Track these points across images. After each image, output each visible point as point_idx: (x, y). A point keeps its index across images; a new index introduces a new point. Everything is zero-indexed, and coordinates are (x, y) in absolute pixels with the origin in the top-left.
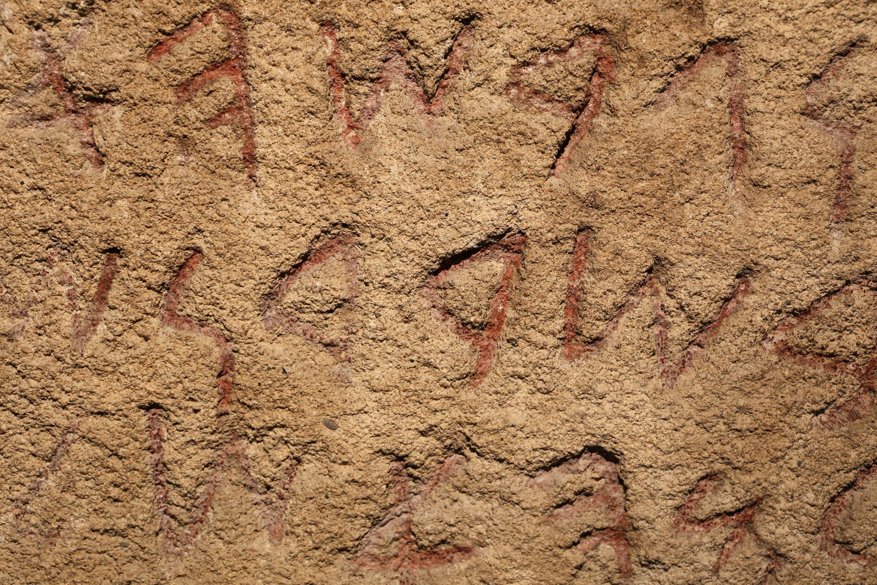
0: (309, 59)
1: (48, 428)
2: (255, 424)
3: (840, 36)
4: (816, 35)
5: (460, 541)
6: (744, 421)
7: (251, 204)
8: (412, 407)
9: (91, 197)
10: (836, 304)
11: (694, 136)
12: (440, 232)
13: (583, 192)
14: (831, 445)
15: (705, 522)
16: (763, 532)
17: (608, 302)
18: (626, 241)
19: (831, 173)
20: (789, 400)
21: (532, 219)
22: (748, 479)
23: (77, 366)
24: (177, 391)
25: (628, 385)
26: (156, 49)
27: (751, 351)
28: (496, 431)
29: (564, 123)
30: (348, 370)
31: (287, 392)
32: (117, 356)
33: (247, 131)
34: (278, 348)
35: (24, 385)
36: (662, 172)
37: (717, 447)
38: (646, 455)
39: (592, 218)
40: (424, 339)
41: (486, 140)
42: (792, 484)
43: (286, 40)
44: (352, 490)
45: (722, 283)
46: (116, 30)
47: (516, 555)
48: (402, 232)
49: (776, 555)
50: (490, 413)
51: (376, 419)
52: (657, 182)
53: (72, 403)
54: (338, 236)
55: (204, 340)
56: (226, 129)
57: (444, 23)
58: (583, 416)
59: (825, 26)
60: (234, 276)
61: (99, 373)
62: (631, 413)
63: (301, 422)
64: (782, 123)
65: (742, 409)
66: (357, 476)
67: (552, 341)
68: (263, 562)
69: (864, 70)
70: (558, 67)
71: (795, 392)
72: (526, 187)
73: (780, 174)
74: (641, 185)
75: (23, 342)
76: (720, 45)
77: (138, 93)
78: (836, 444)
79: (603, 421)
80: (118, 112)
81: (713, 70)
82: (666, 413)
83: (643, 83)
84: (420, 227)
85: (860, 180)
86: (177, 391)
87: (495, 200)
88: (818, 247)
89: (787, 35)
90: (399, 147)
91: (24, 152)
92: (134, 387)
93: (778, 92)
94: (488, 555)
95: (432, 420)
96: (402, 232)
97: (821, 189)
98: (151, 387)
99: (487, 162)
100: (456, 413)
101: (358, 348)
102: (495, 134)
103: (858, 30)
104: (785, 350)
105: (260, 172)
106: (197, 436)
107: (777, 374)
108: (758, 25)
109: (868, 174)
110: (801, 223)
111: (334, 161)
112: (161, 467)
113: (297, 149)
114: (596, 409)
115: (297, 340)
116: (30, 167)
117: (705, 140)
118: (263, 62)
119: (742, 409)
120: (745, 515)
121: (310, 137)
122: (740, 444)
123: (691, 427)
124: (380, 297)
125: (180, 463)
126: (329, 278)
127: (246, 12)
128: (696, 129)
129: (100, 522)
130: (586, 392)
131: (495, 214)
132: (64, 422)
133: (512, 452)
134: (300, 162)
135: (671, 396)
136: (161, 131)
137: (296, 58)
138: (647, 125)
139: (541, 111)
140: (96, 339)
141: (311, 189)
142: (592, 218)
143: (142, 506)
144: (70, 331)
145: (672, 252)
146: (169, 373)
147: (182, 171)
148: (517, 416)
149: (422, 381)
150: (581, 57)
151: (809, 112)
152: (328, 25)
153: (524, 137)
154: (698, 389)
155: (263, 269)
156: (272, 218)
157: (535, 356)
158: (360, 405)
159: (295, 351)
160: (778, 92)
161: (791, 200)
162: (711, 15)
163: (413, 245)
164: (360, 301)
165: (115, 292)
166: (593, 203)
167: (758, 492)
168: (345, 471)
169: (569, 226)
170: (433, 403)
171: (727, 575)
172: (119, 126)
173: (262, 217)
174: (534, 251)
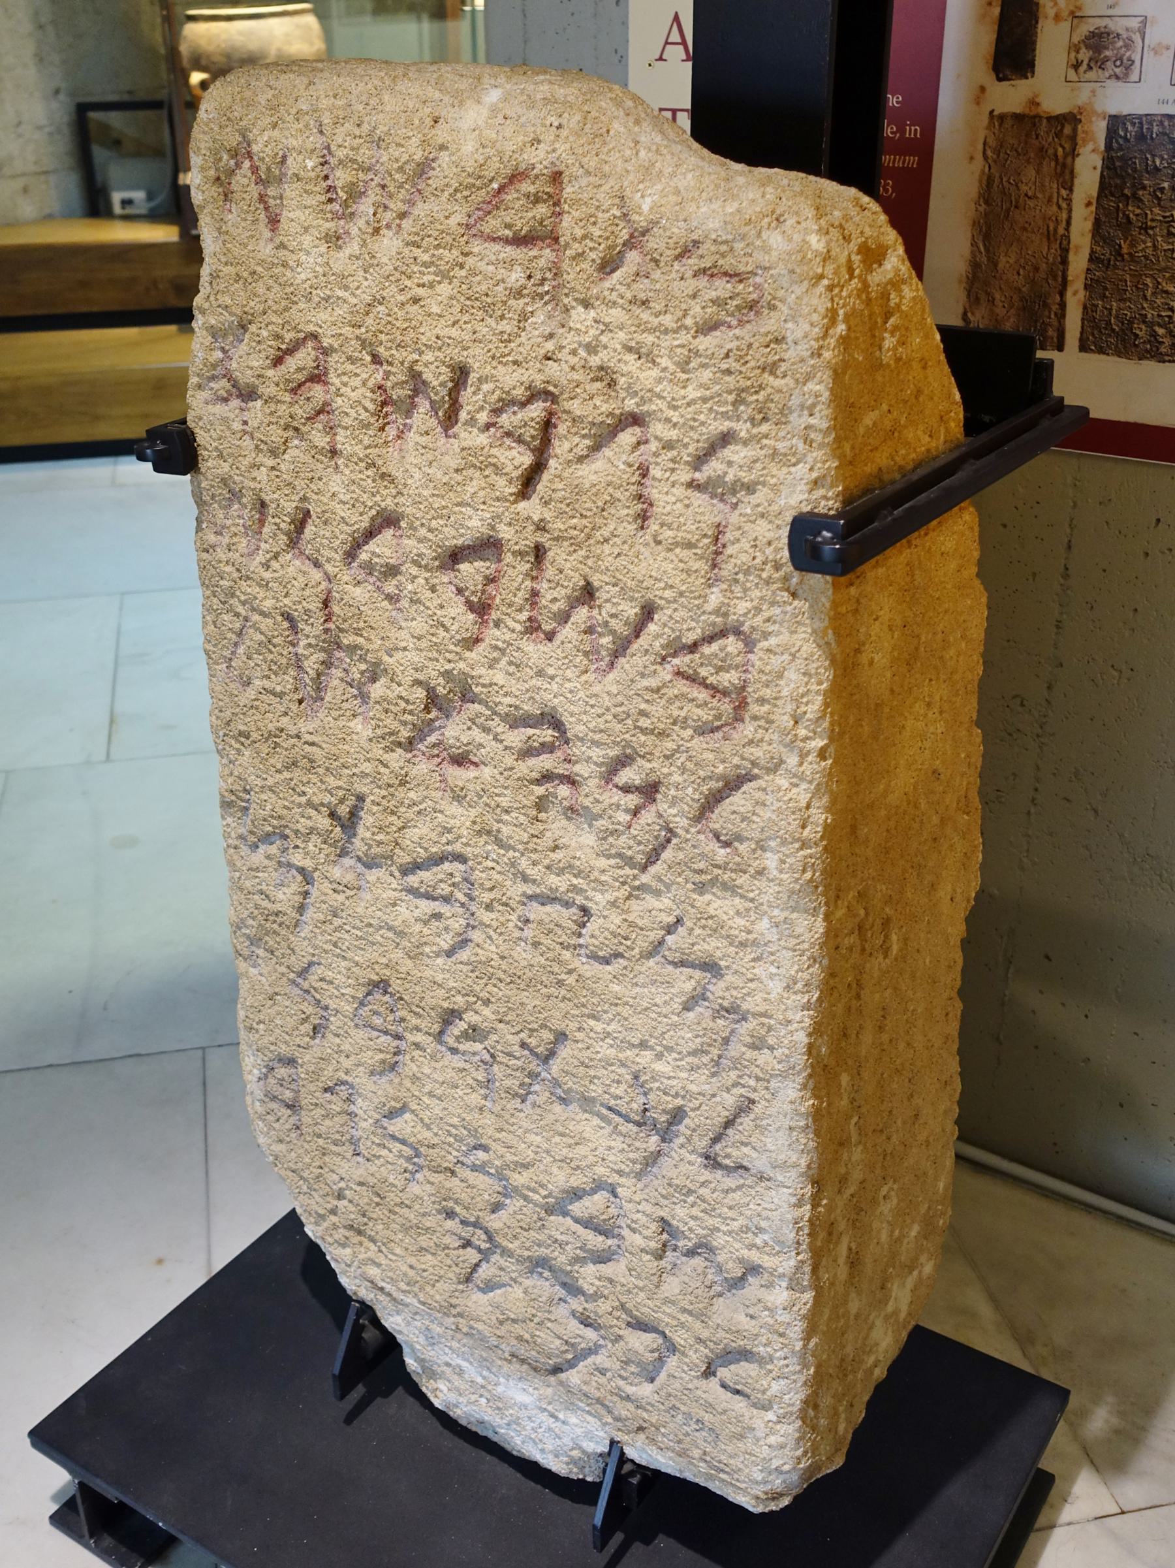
0: (364, 384)
4: (696, 424)
6: (644, 723)
7: (336, 484)
8: (435, 655)
10: (715, 646)
11: (610, 490)
12: (446, 530)
14: (705, 755)
17: (555, 607)
19: (706, 541)
20: (676, 713)
21: (505, 532)
22: (648, 765)
26: (278, 361)
27: (653, 668)
28: (484, 686)
29: (527, 460)
31: (362, 624)
32: (267, 575)
33: (330, 429)
34: (358, 591)
35: (221, 583)
36: (589, 514)
37: (627, 736)
40: (442, 607)
43: (349, 367)
44: (403, 704)
45: (631, 611)
46: (254, 344)
48: (422, 525)
50: (483, 671)
51: (414, 657)
52: (584, 521)
54: (387, 520)
57: (443, 369)
58: (539, 689)
59: (702, 417)
60: (327, 535)
62: (569, 696)
64: (674, 490)
65: (643, 713)
66: (404, 694)
67: (518, 627)
69: (735, 458)
70: (519, 416)
71: (682, 708)
72: (499, 508)
73: (670, 533)
74: (575, 521)
76: (636, 420)
78: (710, 756)
79: (551, 695)
80: (259, 403)
81: (627, 437)
82: (592, 702)
83: (577, 439)
84: (434, 524)
85: (730, 550)
87: (479, 513)
88: (695, 598)
89: (675, 420)
90: (422, 459)
93: (671, 465)
95: (448, 666)
97: (699, 551)
99: (474, 483)
103: (726, 425)
105: (341, 462)
106: (313, 641)
107: (671, 692)
108: (654, 407)
109: (736, 546)
110: (684, 576)
111: (380, 462)
114: (548, 686)
115: (370, 588)
117: (618, 495)
118: (336, 381)
120: (650, 790)
122: (643, 738)
123: (610, 718)
124: (414, 571)
126: (382, 548)
131: (479, 524)
134: (361, 460)
135: (597, 689)
136: (282, 422)
137: (356, 382)
138: (580, 473)
139: (511, 448)
141: (369, 481)
142: (543, 539)
144: (246, 551)
145: (596, 580)
148: (500, 678)
149: (440, 637)
150: (536, 410)
151: (690, 485)
153: (498, 469)
154: (614, 689)
155: (342, 535)
157: (508, 636)
158: (403, 644)
159: (367, 595)
160: (671, 465)
161: (677, 556)
162: (623, 394)
163: (430, 536)
166: (541, 527)
167: (653, 777)
169: (528, 542)
170: (447, 655)
171: (636, 833)
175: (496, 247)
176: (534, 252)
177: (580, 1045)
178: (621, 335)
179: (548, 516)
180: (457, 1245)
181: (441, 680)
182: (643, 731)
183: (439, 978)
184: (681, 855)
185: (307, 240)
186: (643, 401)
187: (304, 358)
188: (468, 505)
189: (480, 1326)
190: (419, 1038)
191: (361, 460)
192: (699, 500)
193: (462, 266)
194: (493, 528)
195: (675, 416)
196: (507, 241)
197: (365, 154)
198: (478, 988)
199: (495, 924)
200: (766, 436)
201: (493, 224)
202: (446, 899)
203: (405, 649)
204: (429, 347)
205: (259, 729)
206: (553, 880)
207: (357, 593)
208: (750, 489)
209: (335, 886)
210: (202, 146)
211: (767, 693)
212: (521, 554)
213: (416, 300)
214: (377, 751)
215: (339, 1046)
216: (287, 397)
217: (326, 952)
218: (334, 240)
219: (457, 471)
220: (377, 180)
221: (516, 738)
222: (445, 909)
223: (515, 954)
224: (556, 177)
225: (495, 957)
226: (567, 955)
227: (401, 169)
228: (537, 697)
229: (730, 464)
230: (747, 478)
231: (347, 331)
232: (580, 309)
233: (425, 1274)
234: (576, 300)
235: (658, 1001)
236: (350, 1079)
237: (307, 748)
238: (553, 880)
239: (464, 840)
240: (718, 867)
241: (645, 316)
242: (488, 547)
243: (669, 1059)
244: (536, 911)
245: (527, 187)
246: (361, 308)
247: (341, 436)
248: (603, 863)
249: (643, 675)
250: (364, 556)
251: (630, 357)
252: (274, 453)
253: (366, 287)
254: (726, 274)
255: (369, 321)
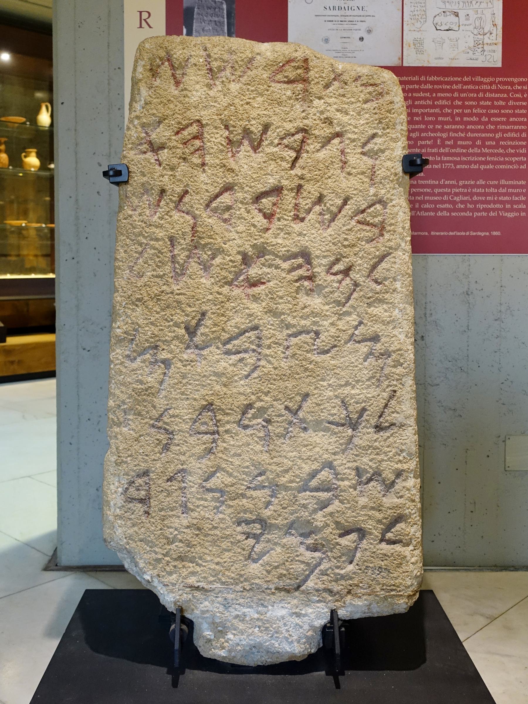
1: (141, 244)
2: (203, 243)
3: (371, 132)
5: (262, 281)
6: (346, 243)
7: (203, 177)
9: (157, 174)
10: (372, 209)
13: (299, 174)
15: (335, 274)
16: (351, 276)
18: (312, 190)
20: (359, 236)
21: (285, 183)
23: (150, 225)
24: (180, 232)
25: (313, 232)
30: (230, 228)
32: (162, 222)
33: (202, 156)
38: (318, 253)
39: (302, 182)
40: (253, 218)
41: (272, 160)
42: (360, 262)
44: (231, 264)
47: (280, 284)
49: (356, 285)
53: (148, 236)
54: (228, 188)
55: (188, 217)
56: (197, 156)
61: (157, 227)
63: (216, 242)
65: (346, 239)
66: (232, 259)
68: (203, 286)
75: (135, 218)
77: (172, 145)
80: (166, 150)
81: (336, 141)
86: (180, 232)
91: (139, 162)
92: (167, 231)
94: (271, 284)
95: (255, 242)
96: (247, 186)
98: (172, 231)
100: (262, 240)
101: (233, 221)
102: (274, 158)
104: (359, 222)
106: (185, 246)
112: (174, 257)
113: (218, 161)
116: (140, 166)
118: (208, 137)
119: (346, 239)
121: (221, 158)
123: (331, 245)
125: (179, 255)
127: (204, 122)
128: (331, 157)
129: (155, 273)
130: (300, 234)
132: (146, 242)
133: (279, 252)
140: (156, 217)
143: (168, 268)
145: (325, 192)
146: (177, 227)
147: (183, 168)
148: (280, 241)
151: (363, 153)
152: (227, 127)
154: (333, 233)
156: (209, 181)
157: (285, 223)
164: (234, 206)
165: (162, 203)
168: (228, 258)
172: (166, 154)
173: (206, 181)
174: (285, 192)
175: (280, 85)
176: (295, 85)
177: (316, 396)
178: (335, 106)
179: (304, 172)
180: (244, 538)
181: (250, 249)
182: (345, 246)
183: (242, 390)
184: (362, 293)
185: (198, 87)
186: (344, 126)
187: (194, 129)
188: (269, 174)
189: (257, 581)
190: (228, 427)
191: (218, 165)
192: (365, 158)
193: (268, 91)
194: (279, 181)
195: (356, 130)
196: (285, 82)
197: (226, 57)
198: (263, 388)
199: (272, 353)
200: (389, 133)
201: (279, 77)
202: (246, 351)
203: (234, 239)
204: (254, 119)
205: (149, 295)
206: (303, 322)
207: (210, 220)
208: (383, 151)
209: (184, 363)
210: (145, 57)
211: (393, 221)
212: (292, 189)
213: (248, 103)
214: (216, 288)
215: (179, 450)
216: (181, 146)
217: (176, 399)
218: (209, 86)
219: (264, 162)
220: (230, 65)
221: (286, 265)
222: (246, 355)
223: (282, 365)
224: (306, 60)
225: (272, 369)
226: (309, 355)
227: (243, 60)
228: (299, 244)
229: (376, 144)
230: (382, 148)
231: (215, 117)
232: (317, 100)
233: (225, 565)
234: (315, 97)
235: (353, 360)
236: (185, 467)
237: (177, 297)
238: (303, 322)
239: (259, 317)
240: (378, 293)
241: (344, 99)
242: (277, 190)
243: (358, 386)
244: (294, 341)
245: (293, 64)
246: (222, 108)
247: (208, 158)
248: (327, 307)
249: (344, 225)
250: (214, 205)
251: (338, 113)
252: (172, 169)
253: (225, 101)
254: (371, 85)
255: (226, 113)
